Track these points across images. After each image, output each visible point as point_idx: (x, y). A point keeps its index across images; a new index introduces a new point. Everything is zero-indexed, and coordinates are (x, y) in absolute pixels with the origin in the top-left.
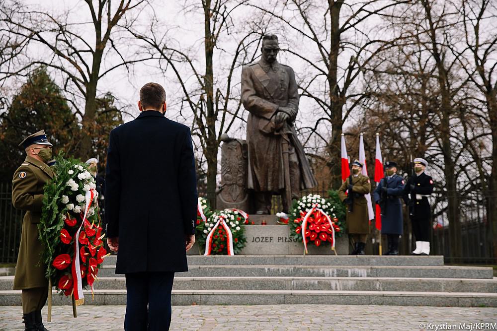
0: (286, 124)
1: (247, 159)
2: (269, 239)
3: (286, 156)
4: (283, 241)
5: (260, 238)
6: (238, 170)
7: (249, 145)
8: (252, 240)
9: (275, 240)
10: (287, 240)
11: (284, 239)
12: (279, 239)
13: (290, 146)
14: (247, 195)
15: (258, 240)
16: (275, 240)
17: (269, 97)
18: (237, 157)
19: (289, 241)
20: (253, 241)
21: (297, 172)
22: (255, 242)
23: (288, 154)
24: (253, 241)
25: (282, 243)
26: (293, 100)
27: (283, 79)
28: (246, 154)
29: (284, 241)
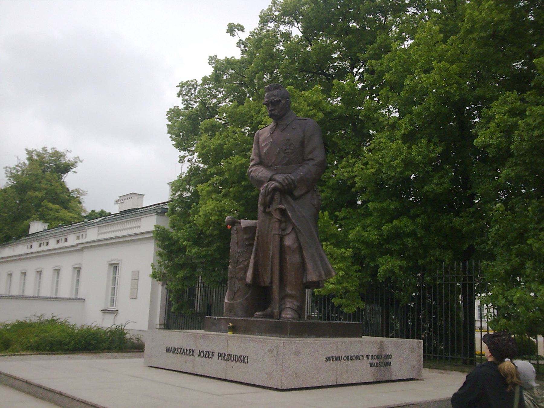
0: (277, 196)
1: (252, 245)
2: (210, 356)
3: (277, 238)
6: (238, 261)
9: (216, 356)
10: (226, 358)
12: (220, 355)
13: (283, 225)
14: (250, 292)
15: (202, 354)
16: (216, 356)
17: (270, 164)
18: (238, 243)
20: (199, 356)
23: (277, 236)
24: (199, 356)
26: (307, 162)
27: (288, 138)
28: (253, 238)
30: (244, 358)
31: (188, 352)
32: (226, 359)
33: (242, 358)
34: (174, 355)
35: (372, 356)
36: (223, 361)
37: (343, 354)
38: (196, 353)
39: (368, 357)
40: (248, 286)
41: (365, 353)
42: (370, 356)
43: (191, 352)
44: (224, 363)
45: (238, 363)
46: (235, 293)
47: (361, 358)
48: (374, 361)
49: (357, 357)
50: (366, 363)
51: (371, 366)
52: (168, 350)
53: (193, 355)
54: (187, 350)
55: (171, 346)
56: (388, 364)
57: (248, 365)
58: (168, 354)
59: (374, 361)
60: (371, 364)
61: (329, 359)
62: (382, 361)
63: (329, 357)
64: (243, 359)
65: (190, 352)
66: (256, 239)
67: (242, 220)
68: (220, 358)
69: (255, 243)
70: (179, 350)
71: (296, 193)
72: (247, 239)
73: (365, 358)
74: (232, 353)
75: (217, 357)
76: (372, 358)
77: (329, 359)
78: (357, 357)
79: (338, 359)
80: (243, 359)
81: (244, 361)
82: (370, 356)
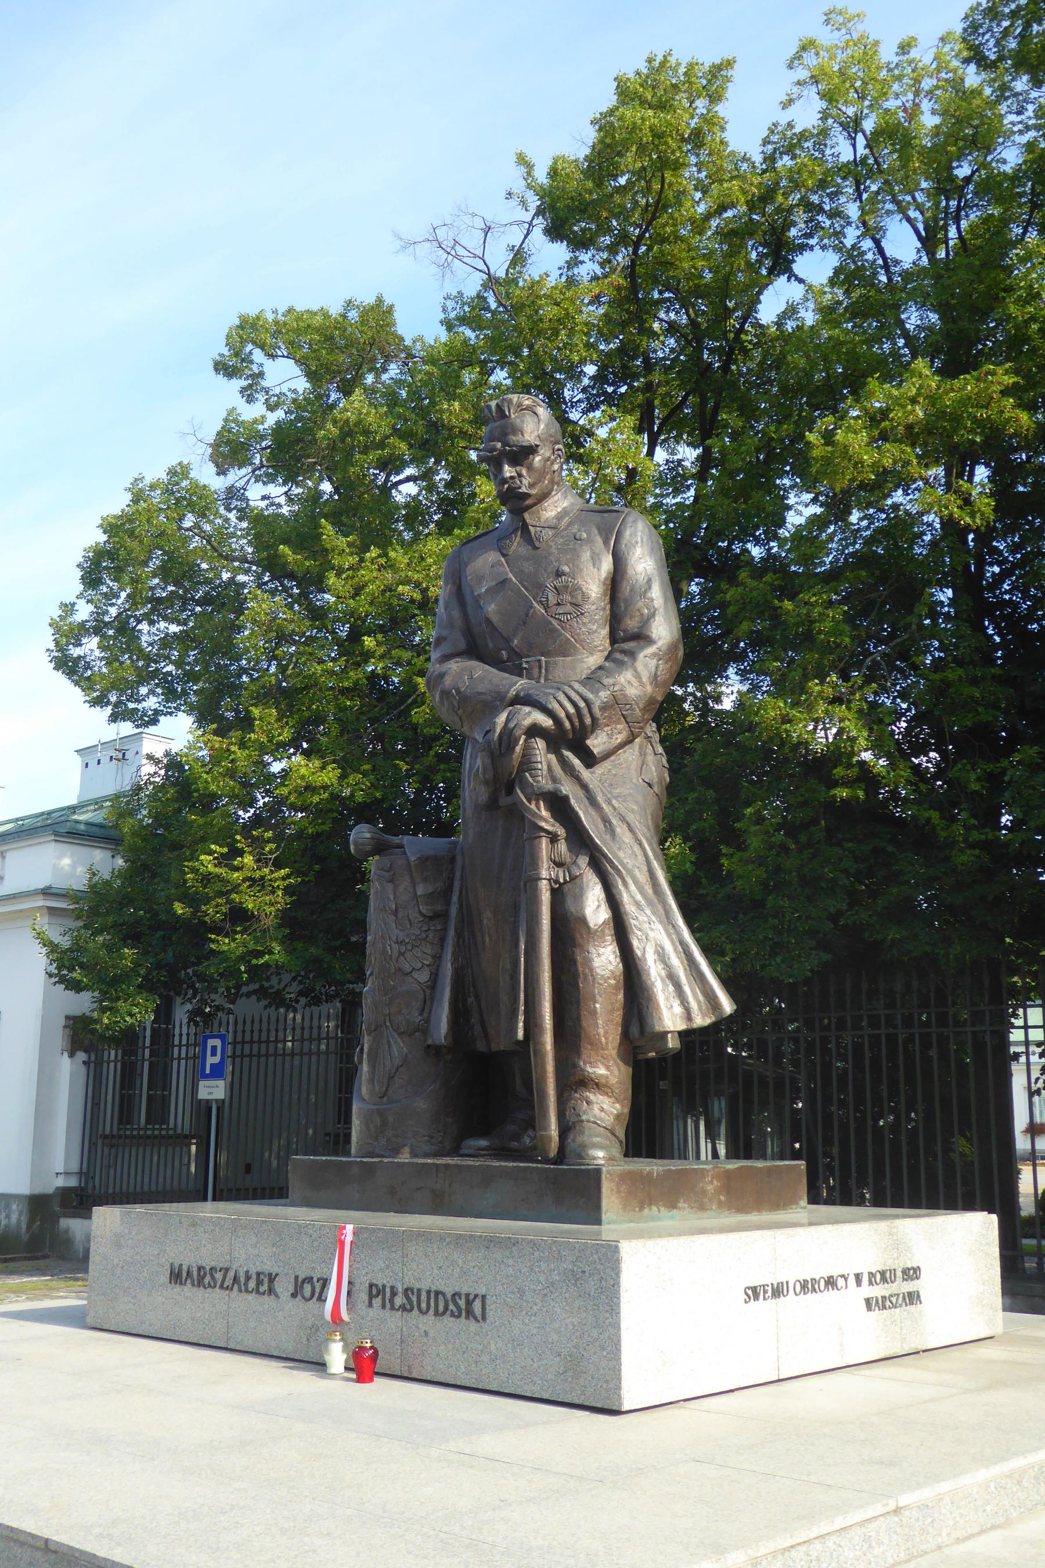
1: (442, 916)
4: (384, 1307)
5: (315, 1279)
7: (459, 859)
8: (291, 1289)
10: (399, 1301)
11: (388, 1290)
15: (307, 1289)
19: (403, 1308)
20: (294, 1295)
21: (604, 959)
22: (299, 1297)
24: (294, 1295)
25: (381, 1312)
26: (626, 646)
28: (445, 894)
29: (388, 1305)
30: (469, 1303)
31: (252, 1284)
32: (403, 1308)
33: (462, 1303)
34: (200, 1292)
35: (871, 1275)
36: (387, 1313)
37: (791, 1275)
38: (285, 1287)
39: (858, 1277)
40: (434, 1051)
41: (851, 1271)
42: (865, 1279)
43: (264, 1283)
44: (394, 1321)
45: (448, 1321)
46: (391, 1078)
47: (841, 1282)
48: (878, 1291)
49: (830, 1282)
50: (855, 1296)
51: (869, 1308)
52: (177, 1276)
53: (271, 1291)
54: (248, 1278)
55: (189, 1260)
56: (913, 1298)
57: (486, 1326)
58: (178, 1288)
59: (878, 1291)
60: (868, 1301)
61: (754, 1293)
62: (896, 1288)
63: (754, 1289)
64: (466, 1307)
65: (259, 1283)
66: (455, 898)
67: (406, 839)
68: (377, 1302)
69: (454, 910)
70: (219, 1276)
71: (597, 743)
72: (431, 897)
73: (852, 1280)
74: (424, 1285)
75: (366, 1298)
76: (871, 1283)
77: (754, 1293)
78: (830, 1282)
79: (778, 1291)
80: (466, 1307)
81: (469, 1313)
82: (865, 1279)
